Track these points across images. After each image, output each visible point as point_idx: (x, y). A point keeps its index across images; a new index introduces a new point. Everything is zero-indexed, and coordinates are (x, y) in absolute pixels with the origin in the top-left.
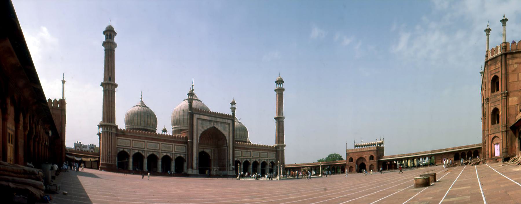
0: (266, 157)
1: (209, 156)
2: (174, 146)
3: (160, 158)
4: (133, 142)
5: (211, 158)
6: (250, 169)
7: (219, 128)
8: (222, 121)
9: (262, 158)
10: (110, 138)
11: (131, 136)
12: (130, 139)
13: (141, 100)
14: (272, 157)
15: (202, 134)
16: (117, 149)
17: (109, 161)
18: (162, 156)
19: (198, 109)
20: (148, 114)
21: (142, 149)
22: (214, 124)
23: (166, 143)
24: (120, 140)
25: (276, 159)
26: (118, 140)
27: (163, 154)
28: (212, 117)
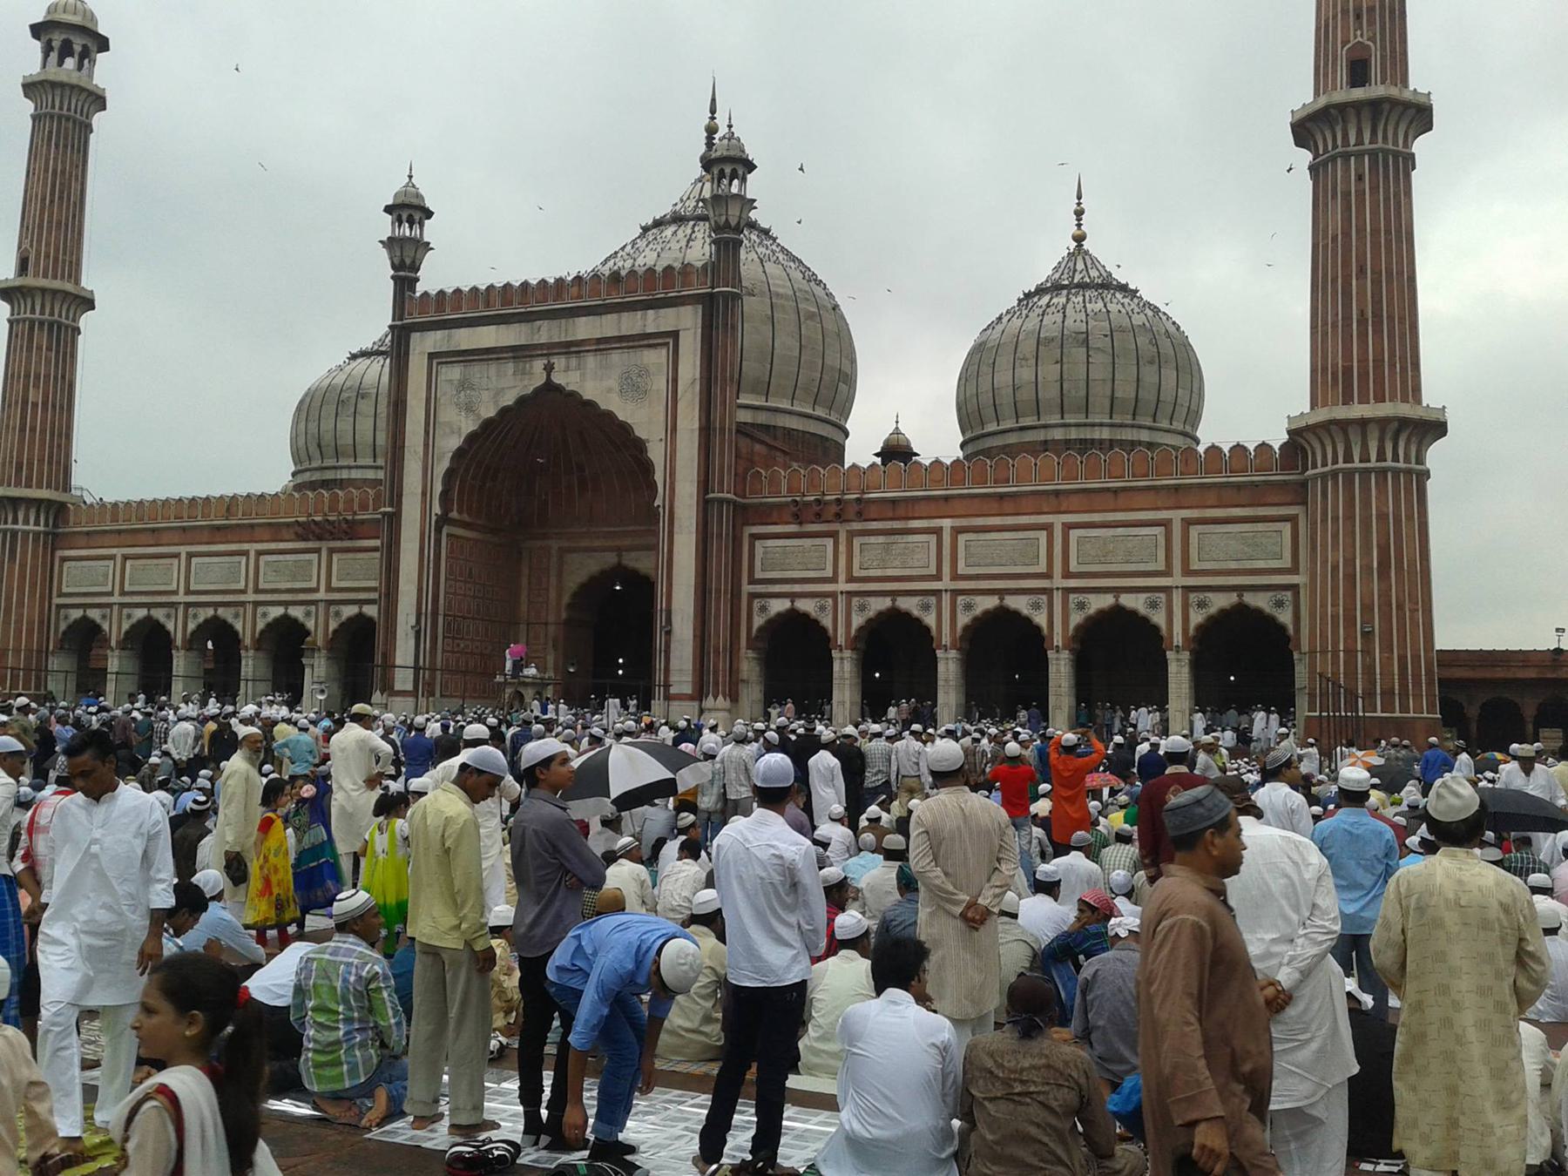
0: (1151, 567)
2: (324, 554)
3: (248, 641)
7: (589, 392)
9: (1073, 583)
12: (114, 551)
14: (1233, 565)
15: (459, 454)
16: (58, 613)
18: (261, 625)
20: (345, 395)
22: (549, 368)
23: (282, 546)
26: (67, 565)
27: (265, 615)
28: (538, 323)
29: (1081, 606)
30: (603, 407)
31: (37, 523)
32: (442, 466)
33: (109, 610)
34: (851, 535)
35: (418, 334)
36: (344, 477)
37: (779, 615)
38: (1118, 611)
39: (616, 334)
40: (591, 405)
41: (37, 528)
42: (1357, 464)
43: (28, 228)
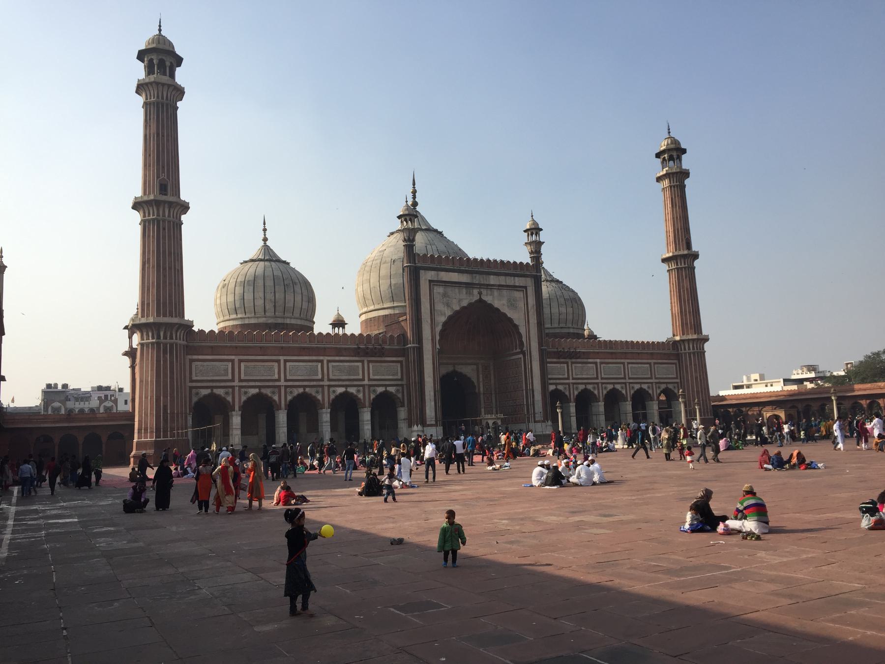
1: (473, 383)
4: (242, 364)
5: (477, 391)
6: (598, 415)
7: (497, 304)
8: (503, 283)
9: (631, 381)
10: (165, 361)
11: (236, 350)
12: (233, 357)
13: (265, 243)
14: (665, 376)
17: (165, 432)
18: (332, 397)
19: (432, 256)
21: (271, 384)
22: (480, 293)
23: (342, 358)
24: (197, 363)
25: (678, 381)
26: (194, 364)
27: (334, 392)
28: (474, 275)
29: (633, 388)
30: (502, 311)
31: (183, 340)
32: (439, 328)
33: (230, 390)
34: (572, 363)
35: (424, 271)
36: (288, 322)
37: (552, 391)
38: (641, 388)
39: (505, 284)
40: (498, 310)
41: (183, 342)
42: (699, 350)
43: (163, 167)
